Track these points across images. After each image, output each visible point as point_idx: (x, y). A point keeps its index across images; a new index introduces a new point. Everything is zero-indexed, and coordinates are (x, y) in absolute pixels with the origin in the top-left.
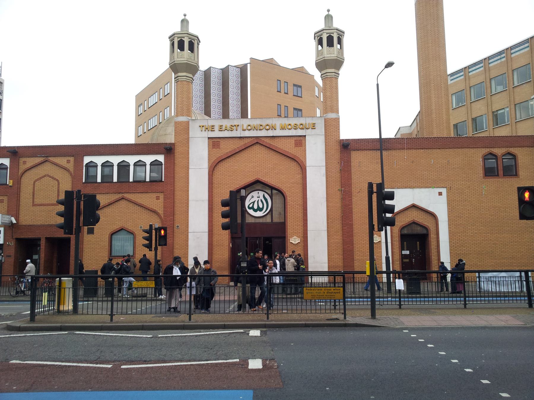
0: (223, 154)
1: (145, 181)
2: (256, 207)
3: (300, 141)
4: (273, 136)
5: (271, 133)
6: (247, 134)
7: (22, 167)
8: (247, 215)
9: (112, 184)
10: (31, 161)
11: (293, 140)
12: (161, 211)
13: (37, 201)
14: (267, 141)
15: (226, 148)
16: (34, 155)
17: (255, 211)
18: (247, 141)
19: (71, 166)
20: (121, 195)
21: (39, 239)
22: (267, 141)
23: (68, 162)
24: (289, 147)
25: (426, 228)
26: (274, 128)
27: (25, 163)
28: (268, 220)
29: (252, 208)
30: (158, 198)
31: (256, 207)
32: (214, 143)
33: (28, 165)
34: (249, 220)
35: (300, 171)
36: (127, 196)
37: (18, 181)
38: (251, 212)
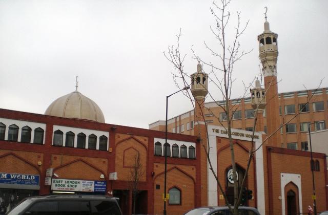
0: (225, 145)
1: (186, 158)
2: (232, 178)
3: (253, 143)
4: (243, 140)
5: (242, 138)
7: (117, 140)
8: (229, 183)
9: (161, 158)
10: (123, 137)
12: (194, 177)
13: (126, 164)
14: (240, 142)
15: (224, 143)
16: (125, 133)
17: (232, 180)
19: (146, 143)
20: (174, 166)
23: (145, 140)
25: (294, 193)
26: (243, 135)
27: (119, 137)
29: (230, 178)
30: (193, 169)
31: (232, 178)
32: (219, 139)
34: (229, 185)
36: (178, 166)
37: (114, 150)
38: (230, 180)
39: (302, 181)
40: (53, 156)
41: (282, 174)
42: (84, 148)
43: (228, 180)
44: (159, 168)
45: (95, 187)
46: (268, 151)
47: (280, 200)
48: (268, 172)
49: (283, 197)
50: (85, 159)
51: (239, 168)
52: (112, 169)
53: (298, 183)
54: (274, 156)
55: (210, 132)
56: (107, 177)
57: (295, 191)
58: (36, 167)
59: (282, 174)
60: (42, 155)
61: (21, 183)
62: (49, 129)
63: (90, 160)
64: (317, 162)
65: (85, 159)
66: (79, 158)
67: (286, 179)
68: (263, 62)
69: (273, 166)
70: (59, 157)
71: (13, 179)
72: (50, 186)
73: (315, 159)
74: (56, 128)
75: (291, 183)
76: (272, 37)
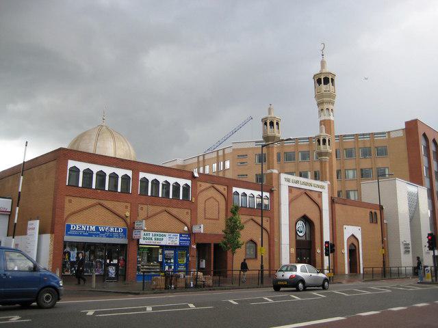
6: (303, 187)
7: (200, 189)
10: (205, 185)
11: (317, 194)
12: (269, 230)
13: (207, 216)
15: (296, 193)
18: (302, 191)
19: (225, 193)
21: (210, 244)
22: (309, 193)
24: (315, 196)
25: (355, 247)
27: (200, 185)
28: (304, 238)
32: (291, 189)
33: (202, 188)
34: (298, 238)
35: (318, 209)
37: (196, 199)
39: (362, 234)
40: (140, 206)
41: (344, 226)
42: (104, 190)
43: (296, 233)
44: (242, 218)
45: (180, 240)
46: (332, 202)
47: (343, 254)
48: (333, 224)
49: (346, 251)
50: (106, 203)
51: (305, 219)
52: (194, 221)
53: (359, 237)
54: (337, 206)
55: (283, 181)
56: (190, 230)
57: (356, 245)
58: (124, 219)
59: (344, 226)
60: (129, 205)
61: (109, 237)
62: (136, 175)
63: (174, 211)
64: (376, 213)
65: (106, 203)
66: (163, 208)
67: (350, 231)
68: (319, 104)
69: (337, 218)
70: (145, 207)
71: (102, 232)
72: (138, 240)
73: (373, 211)
74: (142, 175)
75: (353, 235)
76: (330, 78)
